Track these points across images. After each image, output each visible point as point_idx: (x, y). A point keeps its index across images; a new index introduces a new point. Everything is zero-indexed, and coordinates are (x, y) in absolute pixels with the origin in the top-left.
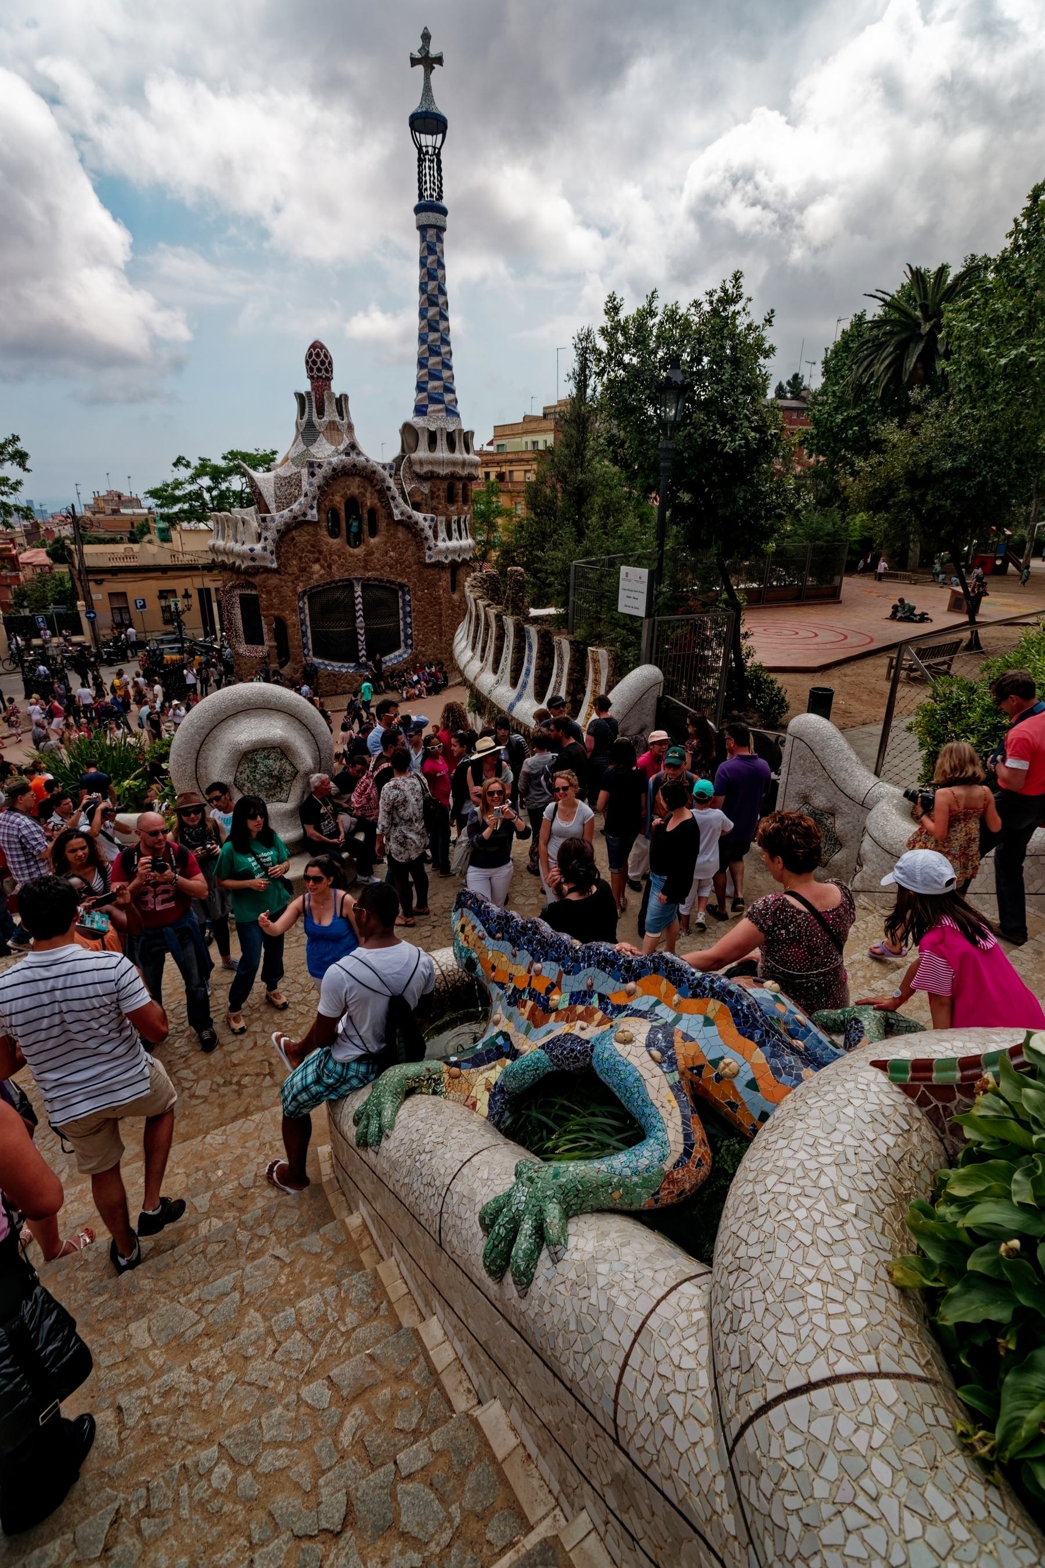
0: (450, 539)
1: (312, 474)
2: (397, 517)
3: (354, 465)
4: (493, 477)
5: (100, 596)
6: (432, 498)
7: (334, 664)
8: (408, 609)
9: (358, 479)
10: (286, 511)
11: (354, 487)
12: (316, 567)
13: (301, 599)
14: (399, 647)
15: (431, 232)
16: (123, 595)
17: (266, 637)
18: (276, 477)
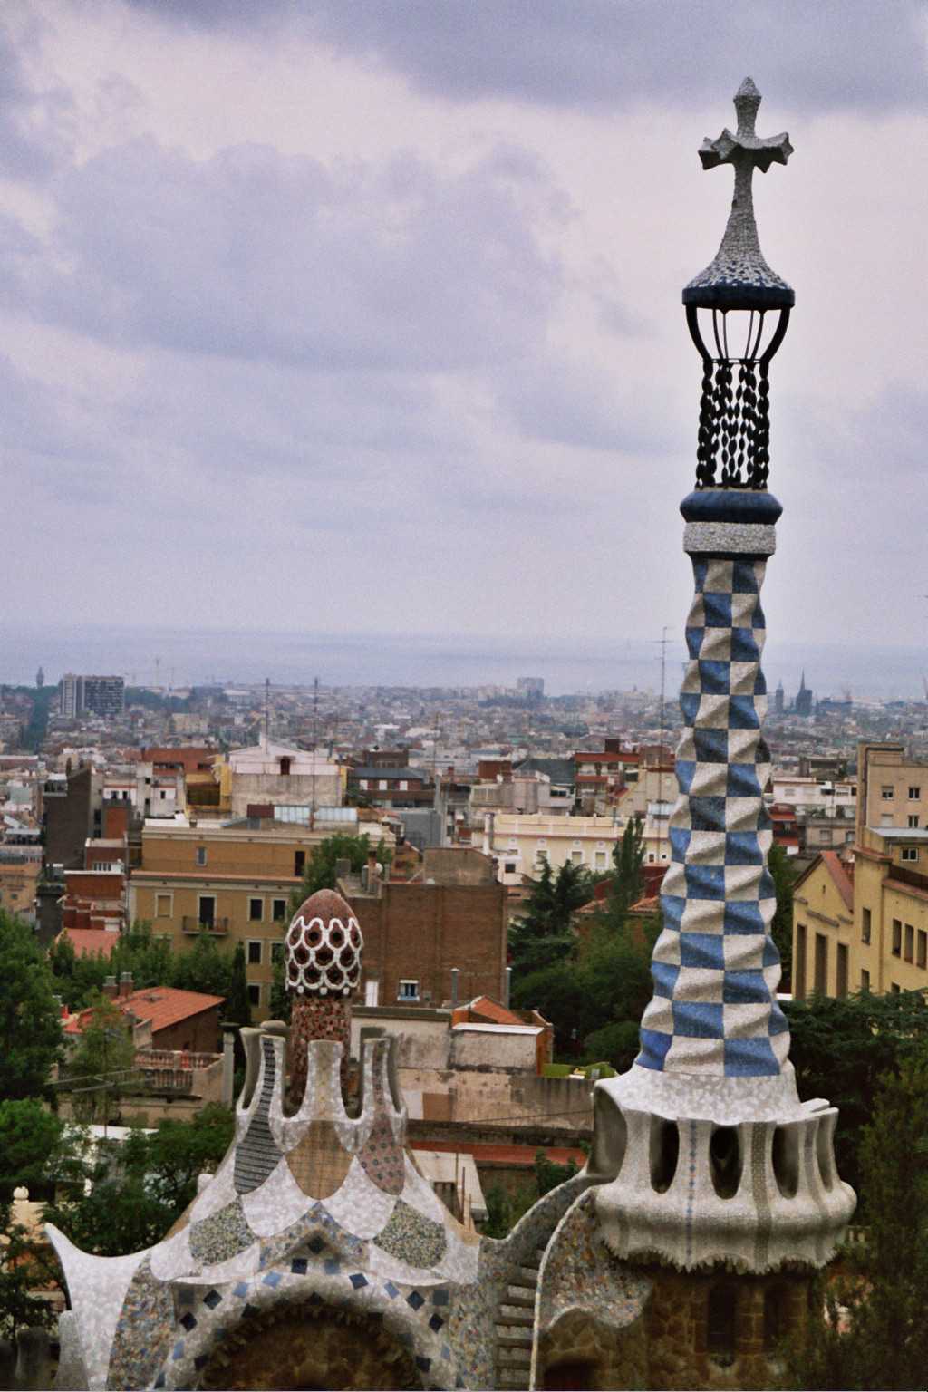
1: (188, 1322)
3: (314, 1298)
6: (656, 1333)
9: (328, 1331)
15: (716, 570)
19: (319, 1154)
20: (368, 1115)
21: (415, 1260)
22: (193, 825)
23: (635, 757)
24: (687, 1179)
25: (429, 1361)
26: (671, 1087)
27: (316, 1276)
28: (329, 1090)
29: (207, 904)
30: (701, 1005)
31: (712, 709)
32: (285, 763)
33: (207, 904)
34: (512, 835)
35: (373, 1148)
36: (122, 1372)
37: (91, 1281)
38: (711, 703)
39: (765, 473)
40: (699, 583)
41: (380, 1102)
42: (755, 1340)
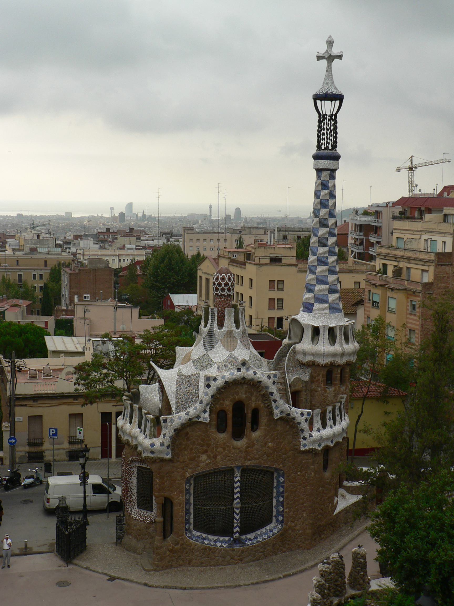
0: (324, 427)
1: (208, 386)
2: (277, 414)
3: (244, 378)
4: (390, 270)
5: (21, 419)
7: (211, 537)
8: (281, 489)
9: (245, 386)
10: (183, 414)
11: (242, 394)
12: (204, 457)
13: (188, 482)
14: (271, 522)
15: (325, 175)
16: (41, 417)
17: (155, 505)
18: (180, 375)
19: (229, 339)
20: (241, 328)
21: (258, 367)
22: (14, 254)
23: (115, 233)
24: (322, 342)
25: (273, 393)
26: (315, 317)
27: (243, 372)
28: (231, 322)
29: (20, 276)
30: (322, 295)
31: (324, 212)
32: (38, 236)
33: (20, 276)
34: (108, 255)
35: (243, 337)
36: (179, 400)
37: (167, 376)
38: (323, 212)
39: (336, 146)
40: (319, 177)
41: (243, 325)
42: (338, 382)
